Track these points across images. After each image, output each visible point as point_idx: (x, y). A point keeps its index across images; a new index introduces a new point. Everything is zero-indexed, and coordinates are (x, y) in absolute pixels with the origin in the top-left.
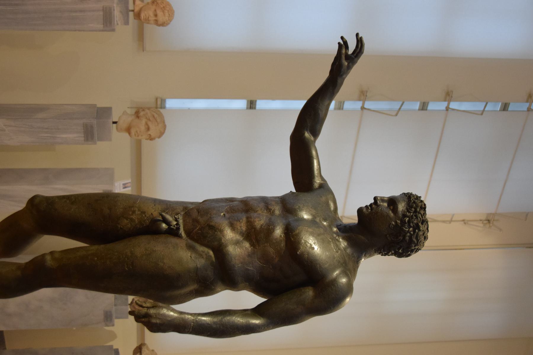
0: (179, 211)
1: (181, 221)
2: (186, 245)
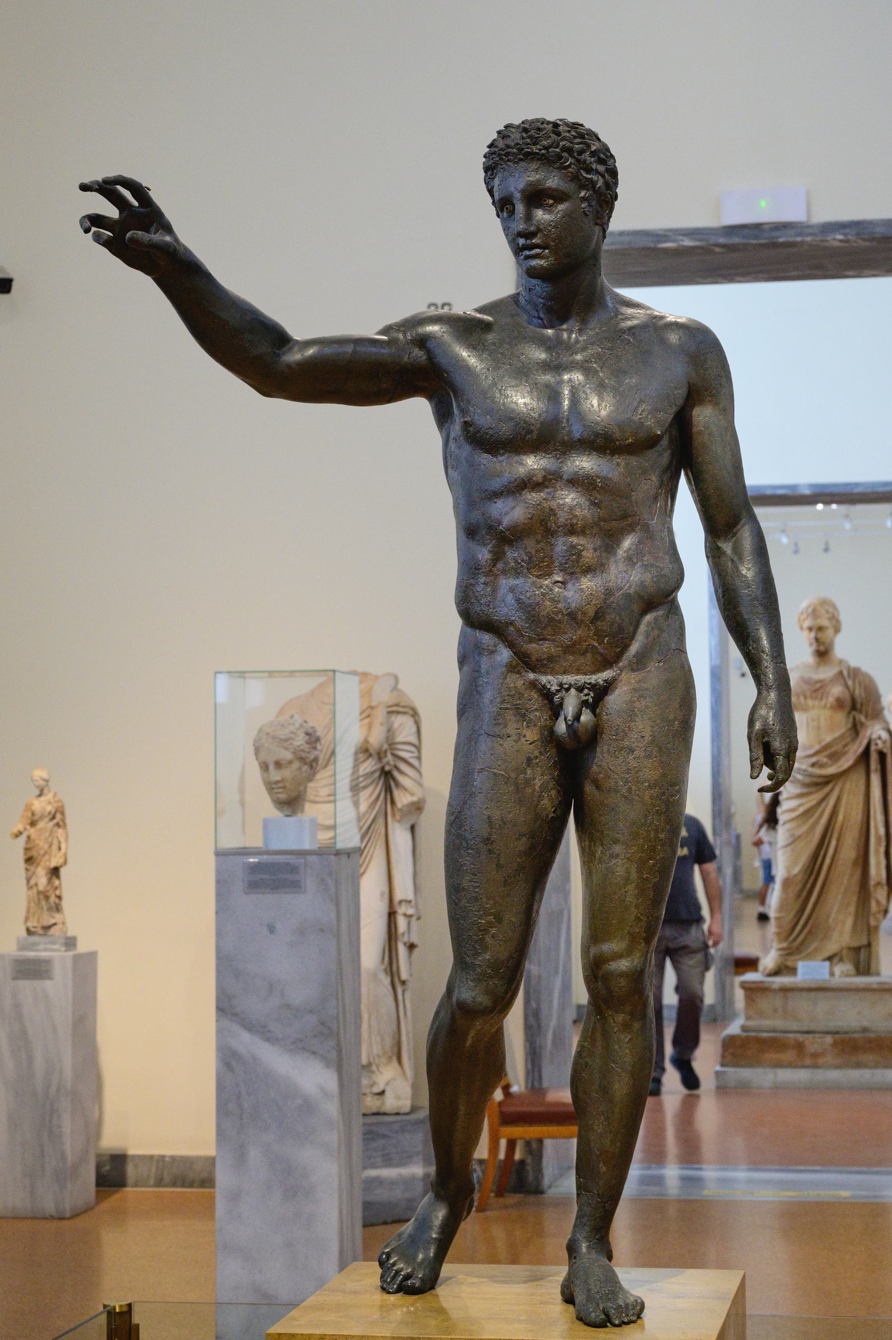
0: (520, 683)
1: (568, 679)
2: (633, 670)
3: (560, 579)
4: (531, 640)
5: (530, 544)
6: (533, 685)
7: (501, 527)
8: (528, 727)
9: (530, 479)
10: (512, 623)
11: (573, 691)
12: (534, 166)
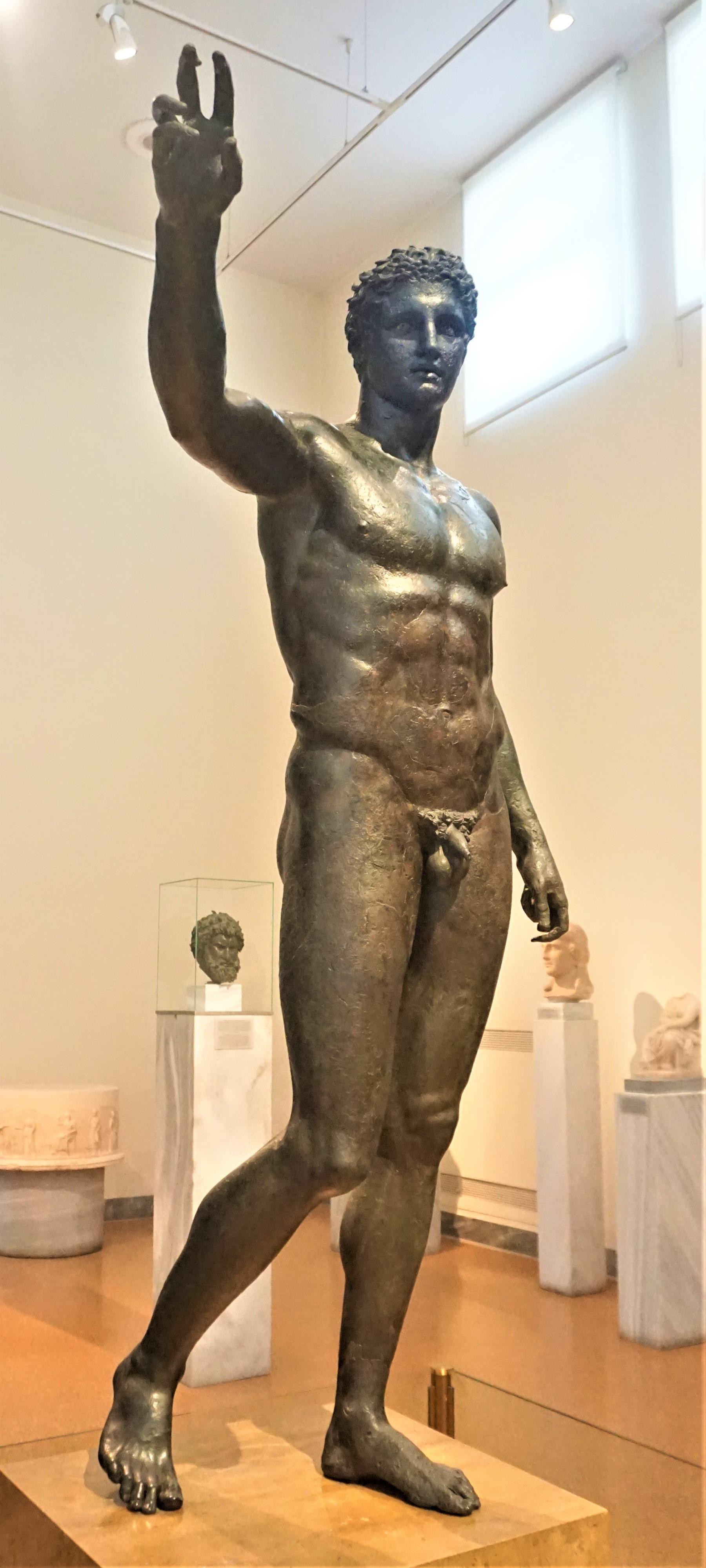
0: (399, 813)
1: (450, 813)
3: (444, 706)
4: (419, 768)
5: (425, 665)
6: (411, 816)
7: (398, 644)
8: (406, 860)
9: (430, 598)
10: (400, 747)
11: (451, 827)
12: (450, 290)
